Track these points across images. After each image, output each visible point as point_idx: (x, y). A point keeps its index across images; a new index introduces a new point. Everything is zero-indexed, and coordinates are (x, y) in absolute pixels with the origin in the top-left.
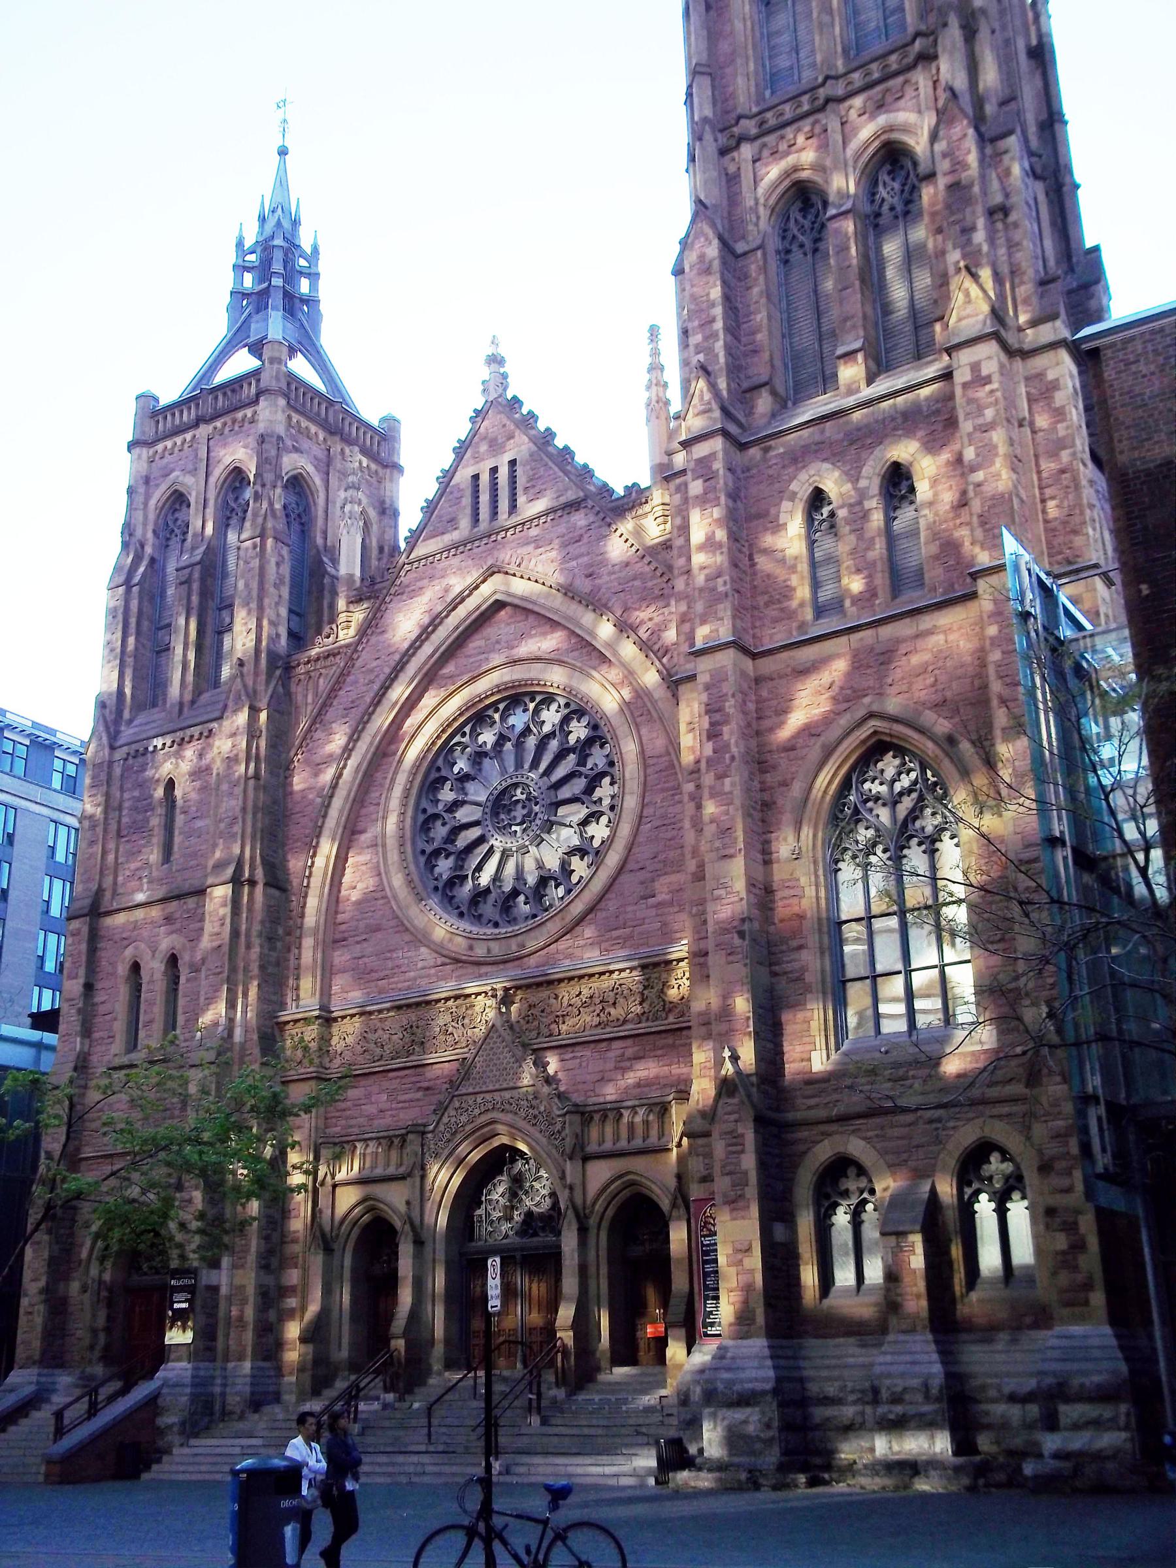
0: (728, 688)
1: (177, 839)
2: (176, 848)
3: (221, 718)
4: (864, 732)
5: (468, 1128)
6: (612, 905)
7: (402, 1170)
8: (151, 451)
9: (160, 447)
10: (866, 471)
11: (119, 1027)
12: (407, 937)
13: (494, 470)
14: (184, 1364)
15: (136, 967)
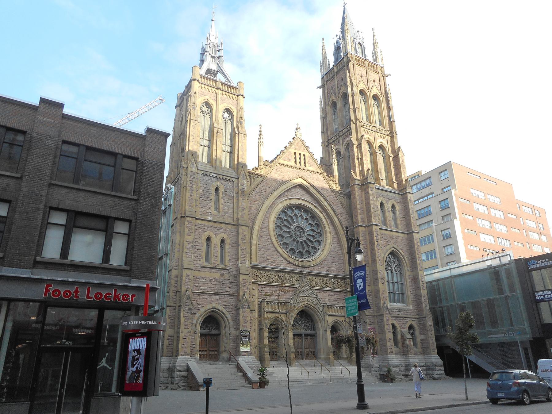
0: (379, 233)
1: (221, 206)
2: (221, 208)
3: (238, 179)
4: (391, 250)
5: (301, 304)
6: (326, 263)
7: (284, 311)
8: (200, 85)
9: (203, 86)
10: (389, 203)
11: (204, 255)
12: (278, 254)
13: (300, 154)
14: (247, 356)
15: (209, 239)
